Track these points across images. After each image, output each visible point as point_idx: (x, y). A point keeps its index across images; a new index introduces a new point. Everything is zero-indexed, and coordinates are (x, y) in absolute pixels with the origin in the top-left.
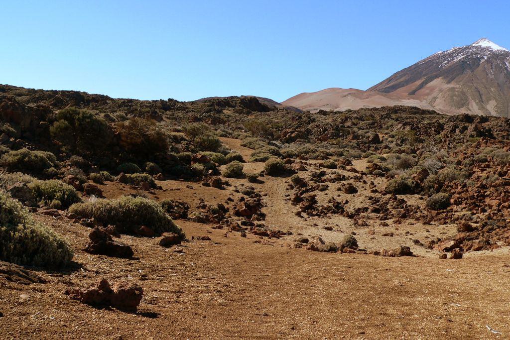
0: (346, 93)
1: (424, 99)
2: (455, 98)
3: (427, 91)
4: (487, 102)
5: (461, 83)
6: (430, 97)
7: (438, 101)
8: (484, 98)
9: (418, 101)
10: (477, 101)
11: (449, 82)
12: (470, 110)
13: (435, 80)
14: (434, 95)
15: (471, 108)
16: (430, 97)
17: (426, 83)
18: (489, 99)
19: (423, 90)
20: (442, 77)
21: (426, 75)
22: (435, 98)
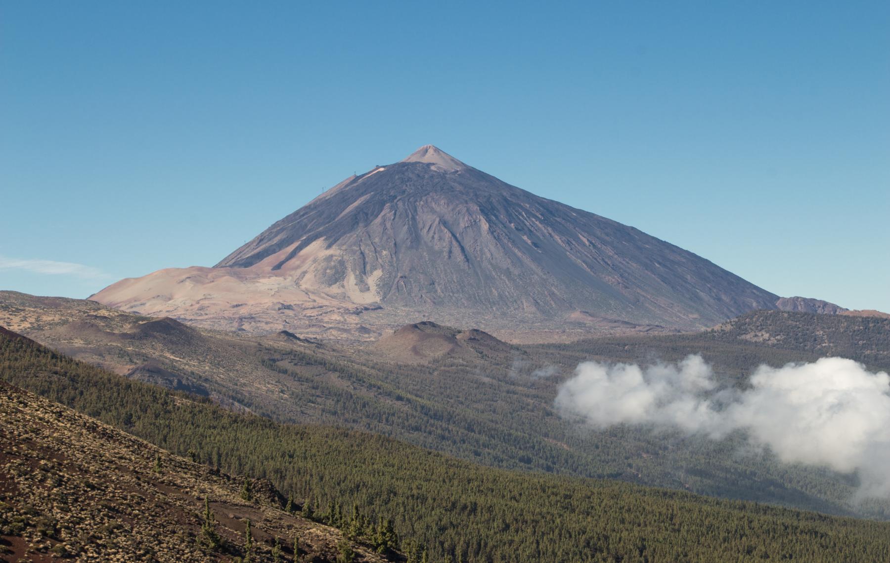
0: (184, 277)
1: (291, 275)
2: (328, 271)
3: (298, 263)
4: (371, 272)
5: (344, 247)
6: (299, 271)
7: (308, 276)
8: (368, 268)
9: (281, 278)
10: (358, 273)
11: (329, 247)
12: (343, 286)
13: (314, 243)
14: (304, 269)
15: (345, 283)
16: (299, 271)
17: (300, 248)
18: (374, 268)
19: (294, 262)
20: (323, 238)
21: (309, 231)
22: (305, 273)
